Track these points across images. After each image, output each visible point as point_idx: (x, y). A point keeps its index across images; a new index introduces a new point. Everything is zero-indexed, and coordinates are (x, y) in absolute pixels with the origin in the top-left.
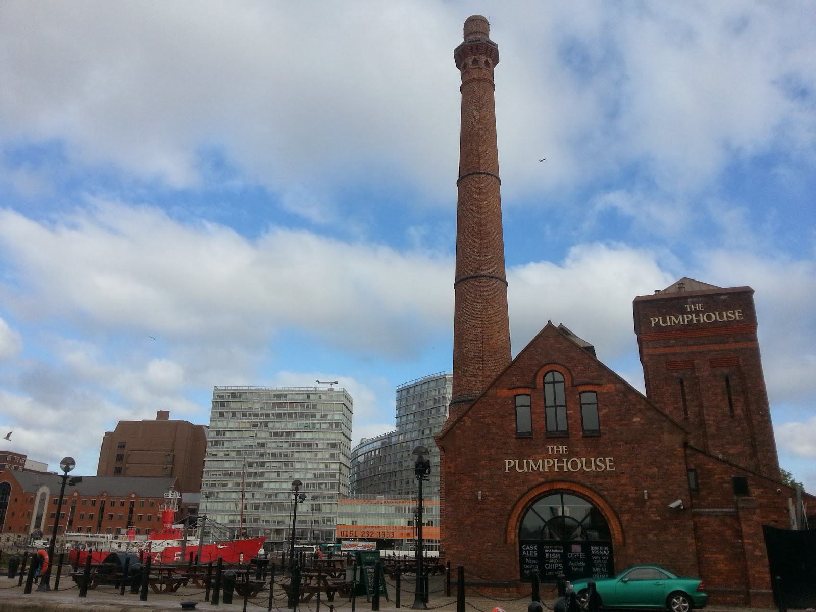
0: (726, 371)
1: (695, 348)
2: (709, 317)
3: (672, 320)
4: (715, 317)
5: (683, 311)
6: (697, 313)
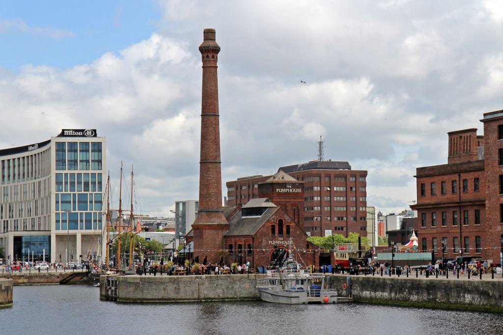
0: (294, 208)
1: (287, 200)
2: (293, 190)
3: (283, 190)
4: (294, 190)
5: (286, 188)
6: (289, 188)
